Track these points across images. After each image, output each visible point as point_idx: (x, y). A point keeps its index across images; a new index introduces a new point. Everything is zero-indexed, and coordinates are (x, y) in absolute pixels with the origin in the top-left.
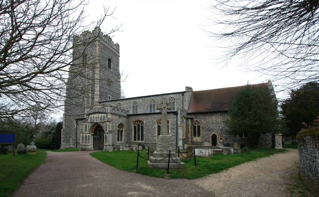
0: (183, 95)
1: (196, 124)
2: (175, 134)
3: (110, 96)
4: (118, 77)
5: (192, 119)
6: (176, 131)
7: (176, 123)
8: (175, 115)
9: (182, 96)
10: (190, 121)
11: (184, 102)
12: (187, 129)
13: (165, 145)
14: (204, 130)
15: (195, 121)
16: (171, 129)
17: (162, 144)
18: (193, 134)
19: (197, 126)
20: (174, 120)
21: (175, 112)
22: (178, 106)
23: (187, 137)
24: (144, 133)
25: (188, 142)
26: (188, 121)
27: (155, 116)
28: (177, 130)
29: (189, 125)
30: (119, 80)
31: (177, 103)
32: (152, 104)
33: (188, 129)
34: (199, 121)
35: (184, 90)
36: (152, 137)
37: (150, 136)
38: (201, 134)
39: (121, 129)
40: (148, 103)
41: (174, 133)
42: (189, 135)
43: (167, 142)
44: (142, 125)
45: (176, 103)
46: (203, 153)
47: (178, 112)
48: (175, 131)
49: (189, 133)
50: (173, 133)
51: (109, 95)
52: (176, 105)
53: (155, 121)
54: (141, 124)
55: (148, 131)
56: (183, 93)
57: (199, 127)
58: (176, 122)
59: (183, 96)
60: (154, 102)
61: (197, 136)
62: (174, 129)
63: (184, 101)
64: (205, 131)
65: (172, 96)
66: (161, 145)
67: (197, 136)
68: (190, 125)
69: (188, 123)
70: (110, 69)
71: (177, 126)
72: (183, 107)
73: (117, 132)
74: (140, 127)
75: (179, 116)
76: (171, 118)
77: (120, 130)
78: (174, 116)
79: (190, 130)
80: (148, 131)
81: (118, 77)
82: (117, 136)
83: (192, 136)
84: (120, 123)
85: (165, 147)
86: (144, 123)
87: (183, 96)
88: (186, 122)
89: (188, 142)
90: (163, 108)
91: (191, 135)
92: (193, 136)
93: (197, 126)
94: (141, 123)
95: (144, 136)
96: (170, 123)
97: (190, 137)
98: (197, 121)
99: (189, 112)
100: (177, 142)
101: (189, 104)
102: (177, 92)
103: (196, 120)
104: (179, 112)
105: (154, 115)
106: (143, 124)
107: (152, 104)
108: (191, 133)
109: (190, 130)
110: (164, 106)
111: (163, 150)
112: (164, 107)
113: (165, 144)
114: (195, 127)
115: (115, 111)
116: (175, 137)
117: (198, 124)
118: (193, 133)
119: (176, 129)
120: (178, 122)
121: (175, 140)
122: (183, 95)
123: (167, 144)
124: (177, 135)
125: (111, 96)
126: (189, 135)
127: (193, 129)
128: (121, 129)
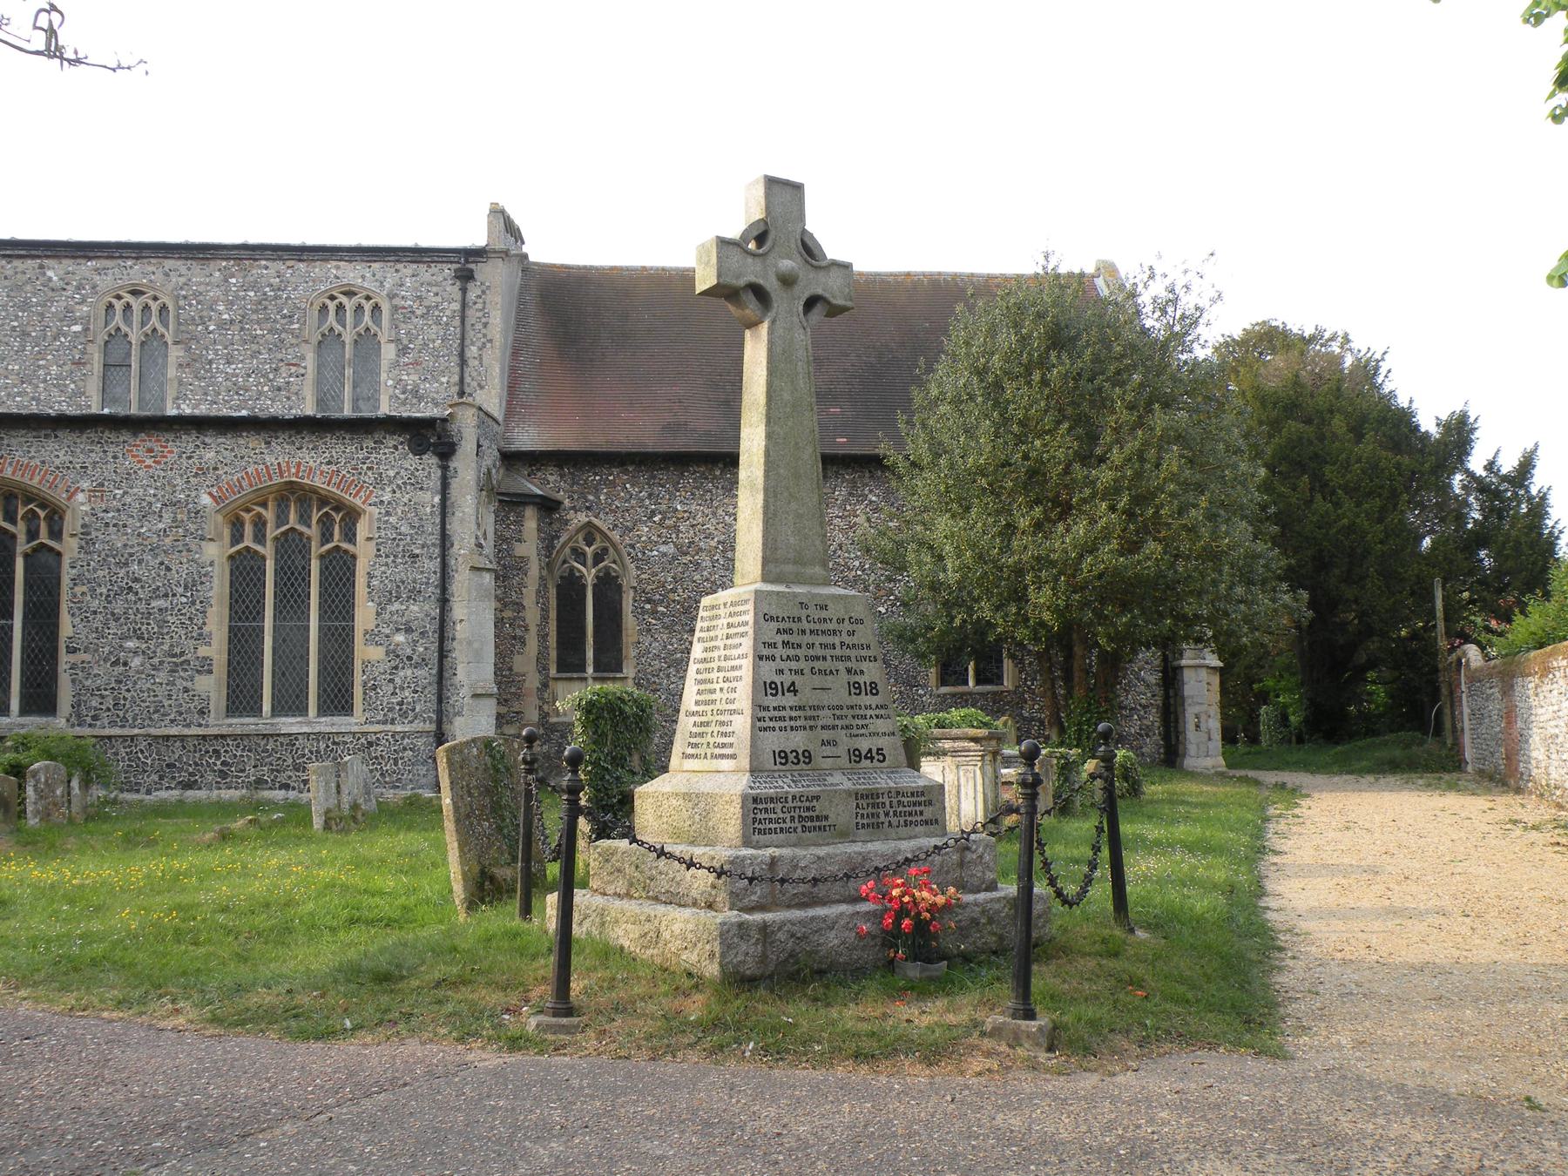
0: (465, 277)
1: (579, 555)
2: (427, 647)
5: (548, 506)
7: (435, 539)
8: (431, 460)
9: (454, 290)
10: (531, 521)
11: (472, 351)
12: (505, 605)
13: (826, 699)
14: (654, 612)
15: (572, 527)
16: (385, 599)
17: (793, 689)
18: (553, 654)
19: (589, 575)
20: (415, 507)
21: (430, 423)
22: (410, 379)
26: (519, 523)
27: (210, 455)
28: (444, 601)
29: (520, 565)
31: (403, 351)
32: (135, 337)
33: (519, 607)
34: (615, 536)
35: (476, 236)
36: (162, 677)
37: (136, 662)
38: (630, 652)
40: (86, 321)
41: (409, 630)
42: (525, 663)
43: (841, 666)
44: (44, 538)
45: (388, 352)
47: (453, 428)
48: (421, 611)
49: (524, 643)
50: (400, 638)
52: (396, 364)
53: (206, 500)
54: (32, 535)
55: (118, 607)
56: (465, 263)
57: (608, 587)
58: (432, 528)
59: (464, 291)
60: (155, 320)
61: (590, 670)
62: (414, 594)
63: (470, 334)
64: (669, 628)
65: (352, 274)
66: (789, 700)
67: (590, 670)
68: (534, 570)
71: (444, 565)
74: (20, 564)
75: (467, 469)
76: (379, 481)
78: (412, 461)
79: (532, 615)
80: (118, 607)
83: (546, 668)
85: (826, 717)
86: (70, 525)
87: (464, 291)
90: (771, 284)
92: (553, 672)
93: (589, 575)
94: (31, 517)
95: (64, 659)
96: (362, 530)
97: (533, 681)
98: (590, 533)
99: (528, 438)
100: (439, 723)
101: (513, 370)
102: (408, 242)
103: (582, 518)
104: (467, 429)
105: (188, 442)
106: (56, 534)
107: (135, 337)
108: (543, 637)
109: (532, 615)
110: (786, 264)
111: (808, 755)
112: (787, 281)
113: (818, 680)
114: (570, 591)
116: (426, 675)
117: (598, 558)
119: (433, 591)
120: (454, 526)
121: (425, 705)
122: (465, 277)
123: (838, 692)
124: (443, 654)
126: (525, 663)
127: (553, 603)
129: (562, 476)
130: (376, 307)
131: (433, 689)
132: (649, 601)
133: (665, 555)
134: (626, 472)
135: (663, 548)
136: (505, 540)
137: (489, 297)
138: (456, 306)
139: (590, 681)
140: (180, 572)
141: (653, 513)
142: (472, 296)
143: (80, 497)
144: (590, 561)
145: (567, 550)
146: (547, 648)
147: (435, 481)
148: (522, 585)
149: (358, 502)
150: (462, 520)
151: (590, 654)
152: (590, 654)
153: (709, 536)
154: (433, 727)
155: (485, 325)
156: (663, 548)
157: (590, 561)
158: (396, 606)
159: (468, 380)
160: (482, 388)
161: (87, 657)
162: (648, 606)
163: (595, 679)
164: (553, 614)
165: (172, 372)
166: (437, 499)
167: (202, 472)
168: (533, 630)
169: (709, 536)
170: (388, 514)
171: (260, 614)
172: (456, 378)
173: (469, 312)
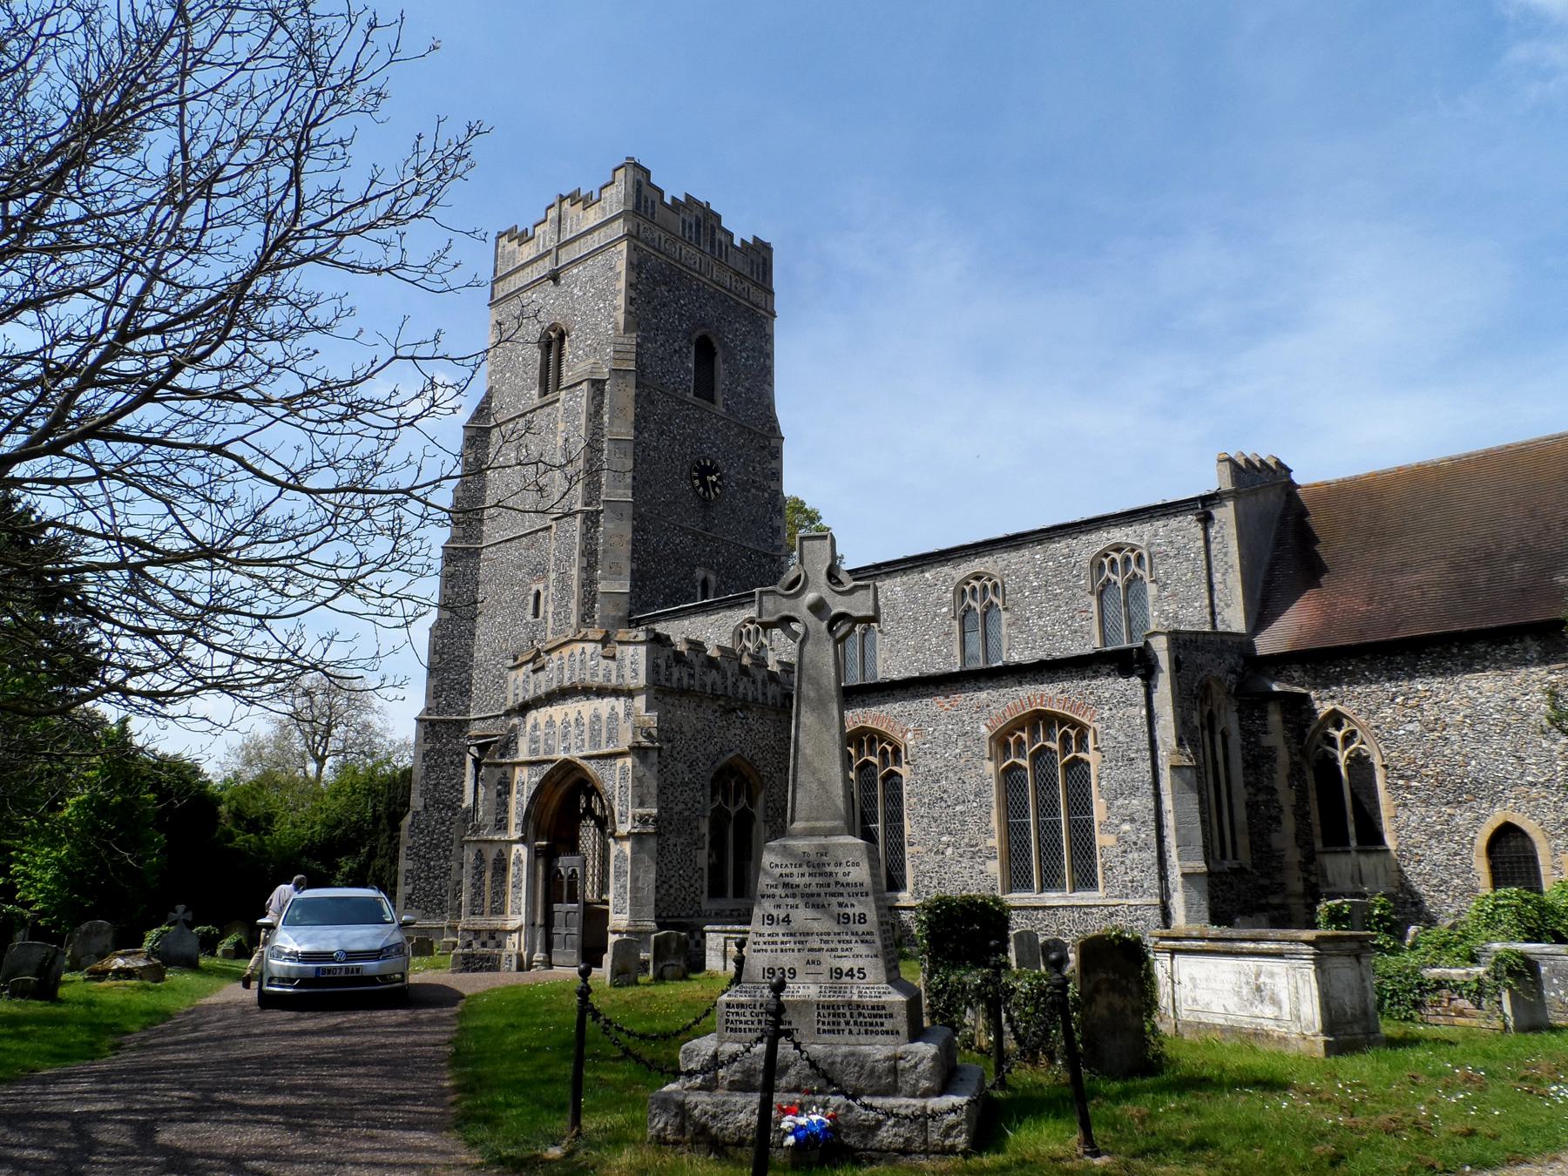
3: (712, 578)
4: (763, 448)
6: (1151, 805)
7: (1145, 744)
8: (1136, 681)
9: (1197, 530)
10: (1275, 718)
11: (1217, 577)
12: (1259, 790)
16: (1113, 796)
18: (1317, 830)
22: (1171, 608)
23: (1265, 855)
24: (907, 830)
25: (1275, 900)
26: (1264, 717)
29: (1269, 755)
30: (774, 464)
33: (1272, 791)
34: (1362, 719)
35: (1212, 480)
36: (966, 862)
39: (743, 801)
41: (1133, 820)
45: (1152, 590)
46: (1275, 1001)
49: (1279, 822)
50: (1126, 827)
51: (700, 573)
52: (1159, 598)
53: (983, 729)
55: (936, 812)
56: (1203, 507)
59: (1206, 530)
61: (1353, 843)
62: (1134, 790)
64: (1426, 802)
65: (1118, 535)
67: (1353, 843)
68: (1283, 756)
69: (1267, 741)
70: (713, 401)
72: (1213, 614)
73: (705, 828)
77: (733, 811)
80: (936, 812)
81: (763, 448)
82: (703, 858)
84: (731, 755)
88: (1246, 733)
89: (1275, 900)
91: (1303, 838)
92: (1319, 845)
95: (908, 849)
97: (1293, 855)
101: (1267, 583)
108: (1301, 815)
115: (691, 676)
116: (1151, 856)
118: (1315, 817)
119: (1148, 787)
120: (1158, 734)
122: (1206, 520)
125: (717, 573)
127: (1311, 783)
128: (743, 801)
129: (1305, 672)
130: (1140, 557)
131: (1155, 869)
132: (1401, 777)
133: (1411, 732)
134: (1363, 661)
135: (1410, 727)
136: (1252, 734)
137: (1225, 532)
138: (1201, 543)
139: (1354, 854)
140: (972, 784)
141: (1395, 696)
142: (1212, 532)
143: (909, 735)
144: (1340, 744)
145: (1319, 736)
146: (1310, 825)
147: (1141, 699)
148: (1272, 771)
149: (1085, 720)
150: (1164, 727)
151: (1352, 829)
152: (1352, 829)
153: (1454, 711)
154: (1157, 901)
155: (1226, 554)
156: (1410, 727)
157: (1340, 744)
158: (1120, 802)
159: (1216, 601)
160: (1228, 606)
161: (919, 848)
162: (1401, 782)
163: (1358, 852)
164: (1313, 795)
165: (1004, 630)
166: (1144, 712)
167: (980, 709)
168: (1288, 810)
169: (1454, 711)
170: (1108, 727)
171: (1056, 813)
172: (1207, 601)
173: (1213, 546)
